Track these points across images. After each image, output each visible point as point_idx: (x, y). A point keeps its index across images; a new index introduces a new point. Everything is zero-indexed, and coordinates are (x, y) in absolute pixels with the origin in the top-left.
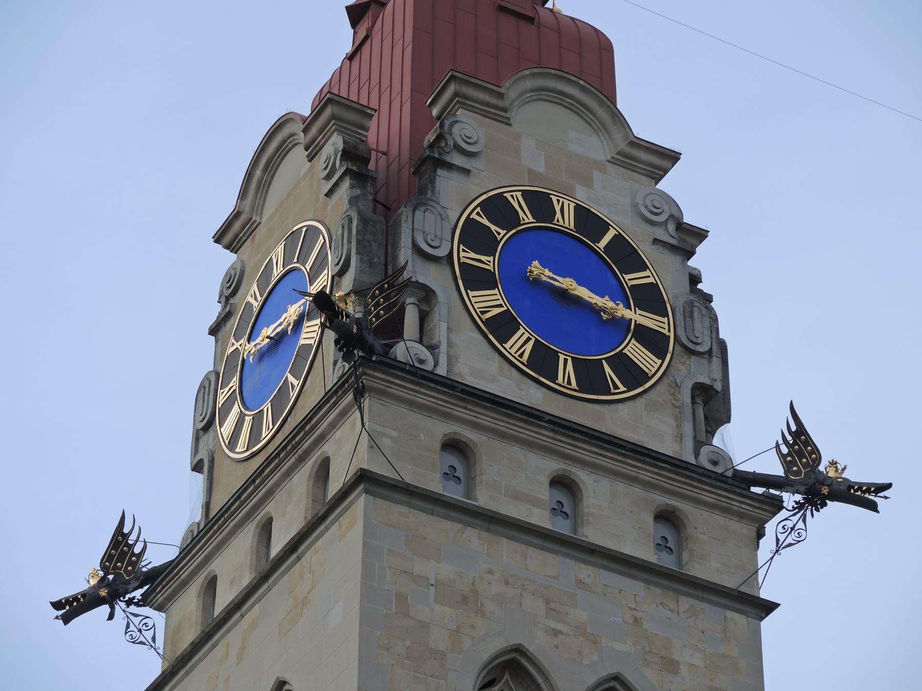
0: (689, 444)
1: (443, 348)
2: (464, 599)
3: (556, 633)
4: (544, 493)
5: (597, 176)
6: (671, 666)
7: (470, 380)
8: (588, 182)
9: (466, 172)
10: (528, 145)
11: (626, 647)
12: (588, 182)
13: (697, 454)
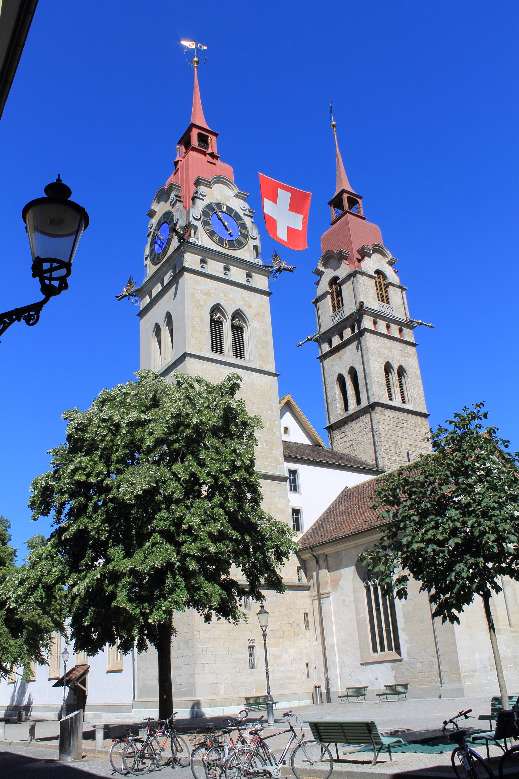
0: (253, 258)
1: (200, 239)
2: (207, 294)
3: (226, 300)
4: (222, 269)
5: (231, 199)
6: (250, 307)
7: (205, 246)
8: (229, 201)
9: (203, 200)
10: (216, 193)
11: (241, 303)
12: (229, 201)
13: (255, 261)
